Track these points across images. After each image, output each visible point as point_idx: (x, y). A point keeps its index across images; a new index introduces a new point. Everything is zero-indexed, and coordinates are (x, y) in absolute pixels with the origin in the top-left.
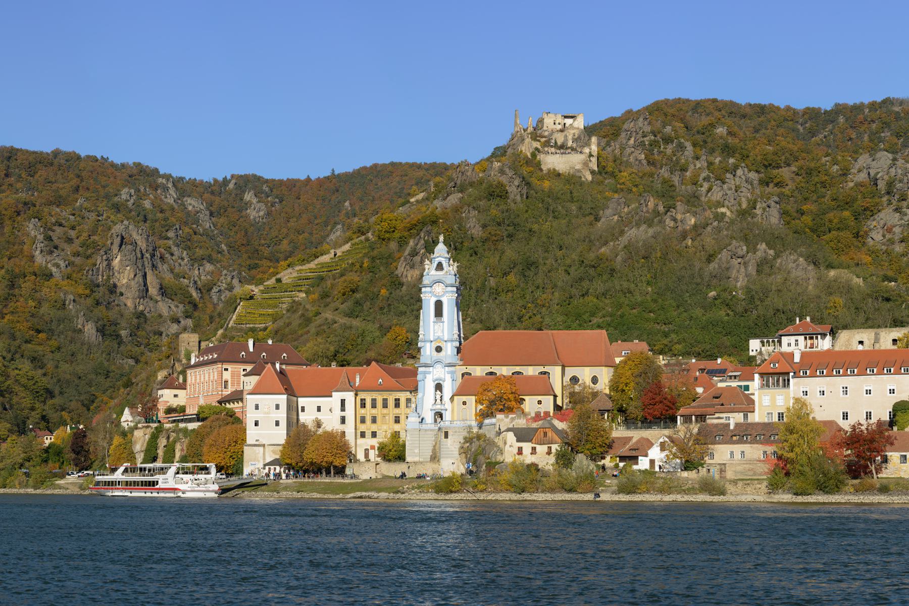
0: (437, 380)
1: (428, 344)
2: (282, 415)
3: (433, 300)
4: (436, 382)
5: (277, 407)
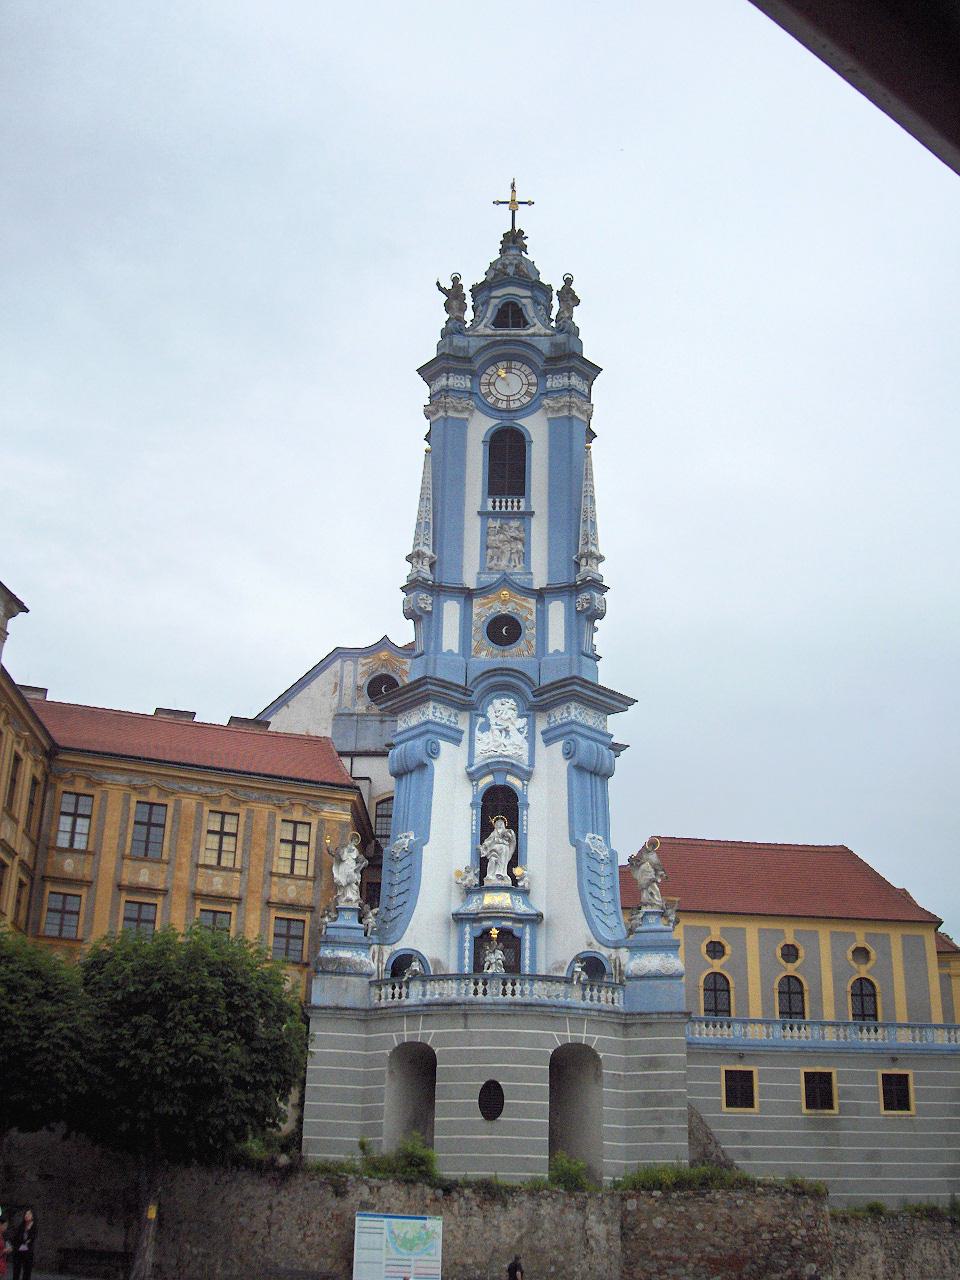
0: (488, 769)
1: (451, 610)
3: (480, 427)
4: (488, 780)
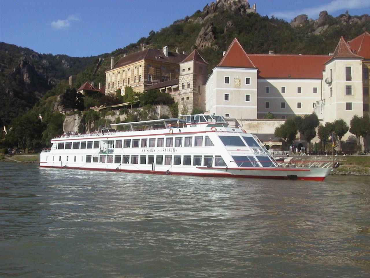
2: (252, 89)
5: (248, 81)
